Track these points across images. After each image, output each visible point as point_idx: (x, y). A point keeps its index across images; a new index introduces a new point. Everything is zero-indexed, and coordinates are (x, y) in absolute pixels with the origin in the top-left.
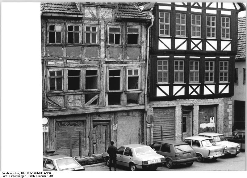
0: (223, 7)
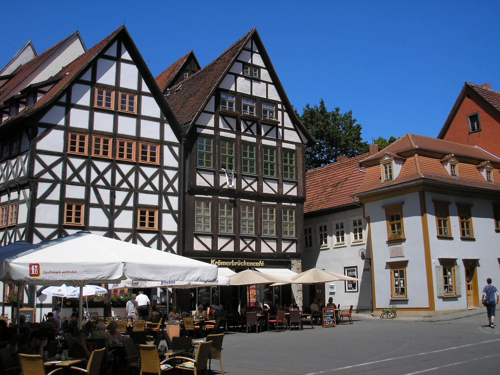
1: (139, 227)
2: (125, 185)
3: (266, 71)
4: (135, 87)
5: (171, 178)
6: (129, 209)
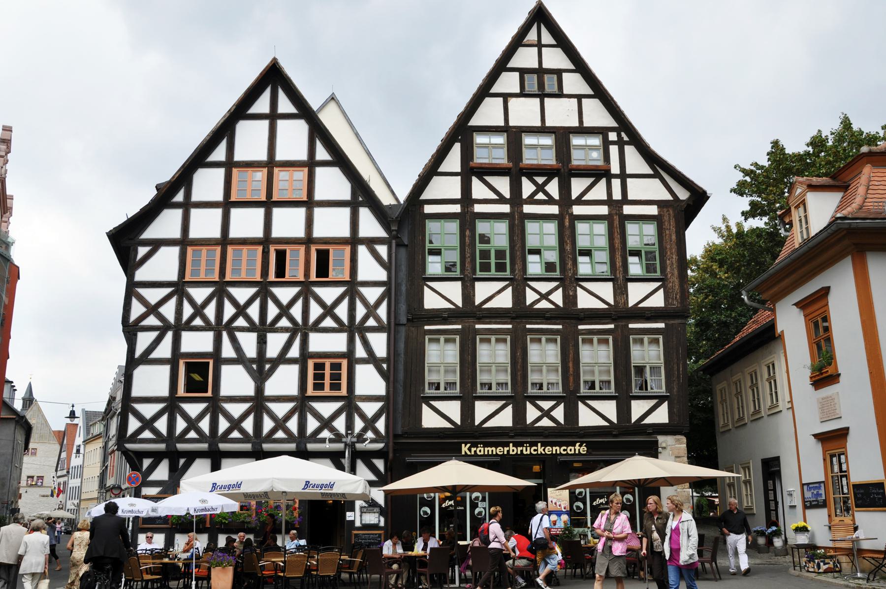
0: (631, 197)
1: (310, 392)
2: (284, 322)
3: (577, 77)
4: (303, 156)
5: (372, 300)
6: (292, 361)
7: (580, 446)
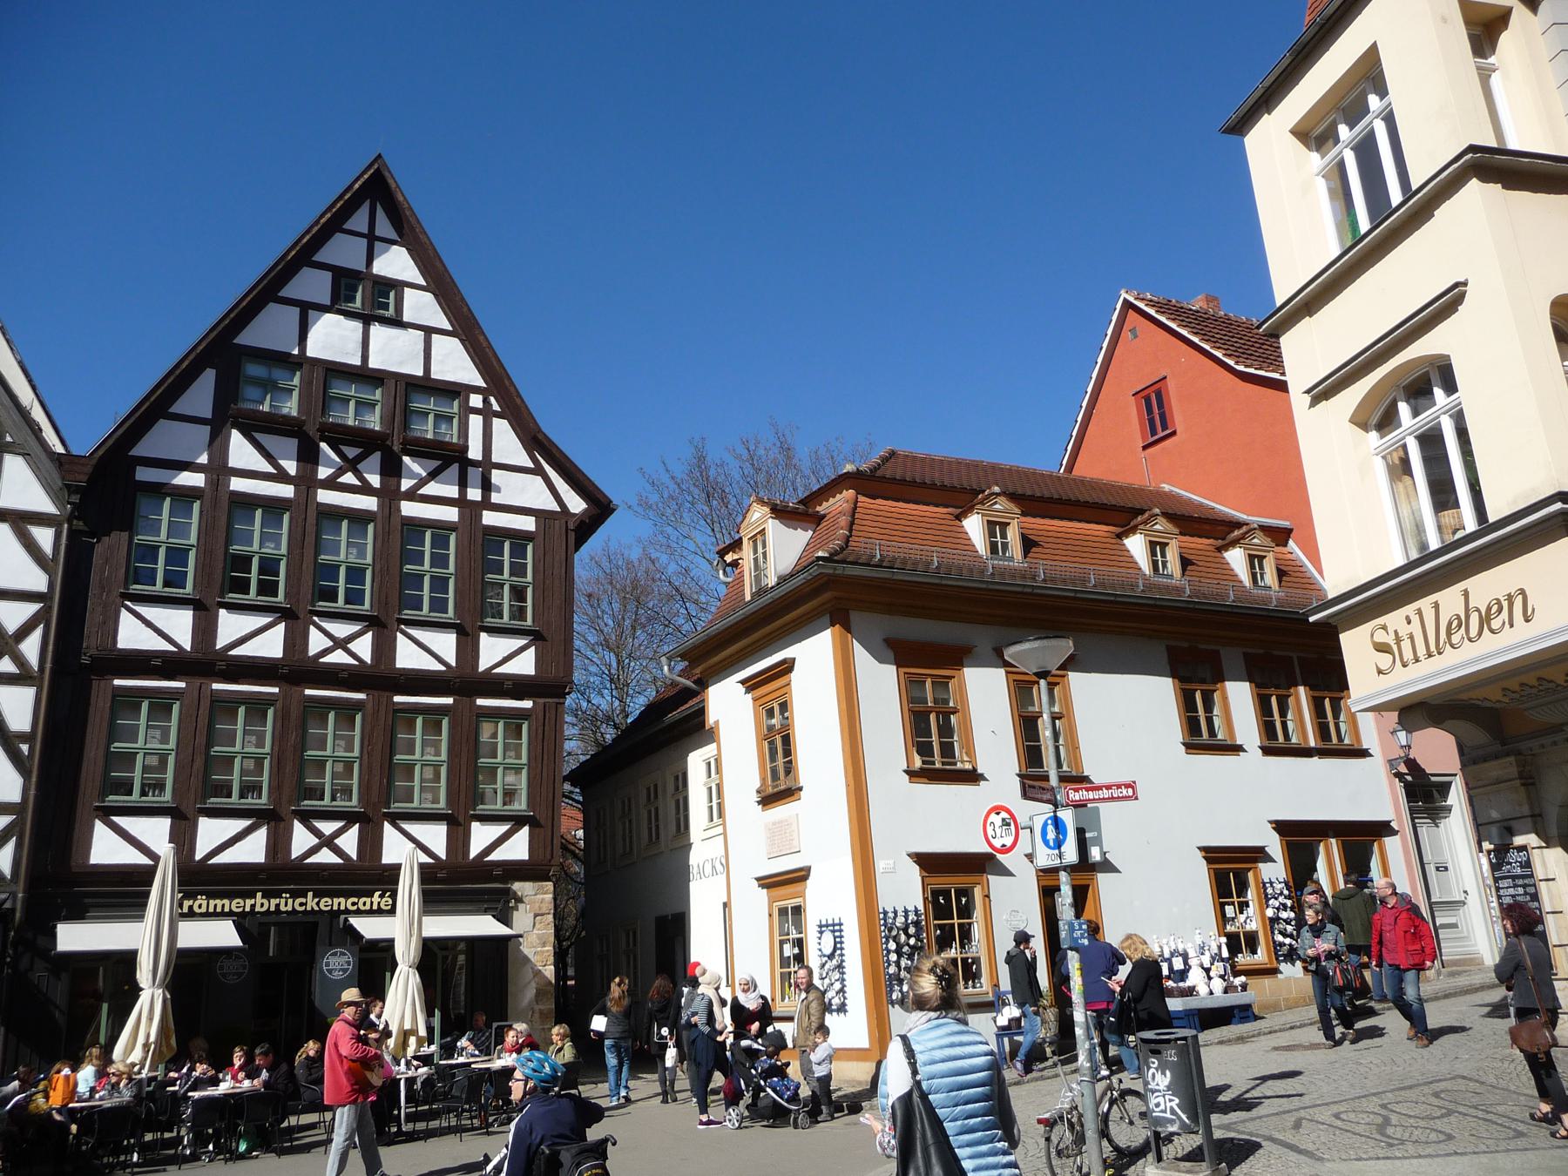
7: (382, 896)
